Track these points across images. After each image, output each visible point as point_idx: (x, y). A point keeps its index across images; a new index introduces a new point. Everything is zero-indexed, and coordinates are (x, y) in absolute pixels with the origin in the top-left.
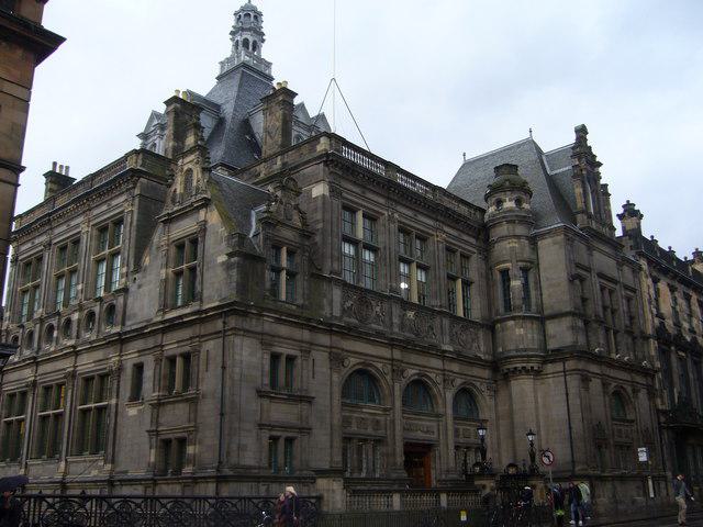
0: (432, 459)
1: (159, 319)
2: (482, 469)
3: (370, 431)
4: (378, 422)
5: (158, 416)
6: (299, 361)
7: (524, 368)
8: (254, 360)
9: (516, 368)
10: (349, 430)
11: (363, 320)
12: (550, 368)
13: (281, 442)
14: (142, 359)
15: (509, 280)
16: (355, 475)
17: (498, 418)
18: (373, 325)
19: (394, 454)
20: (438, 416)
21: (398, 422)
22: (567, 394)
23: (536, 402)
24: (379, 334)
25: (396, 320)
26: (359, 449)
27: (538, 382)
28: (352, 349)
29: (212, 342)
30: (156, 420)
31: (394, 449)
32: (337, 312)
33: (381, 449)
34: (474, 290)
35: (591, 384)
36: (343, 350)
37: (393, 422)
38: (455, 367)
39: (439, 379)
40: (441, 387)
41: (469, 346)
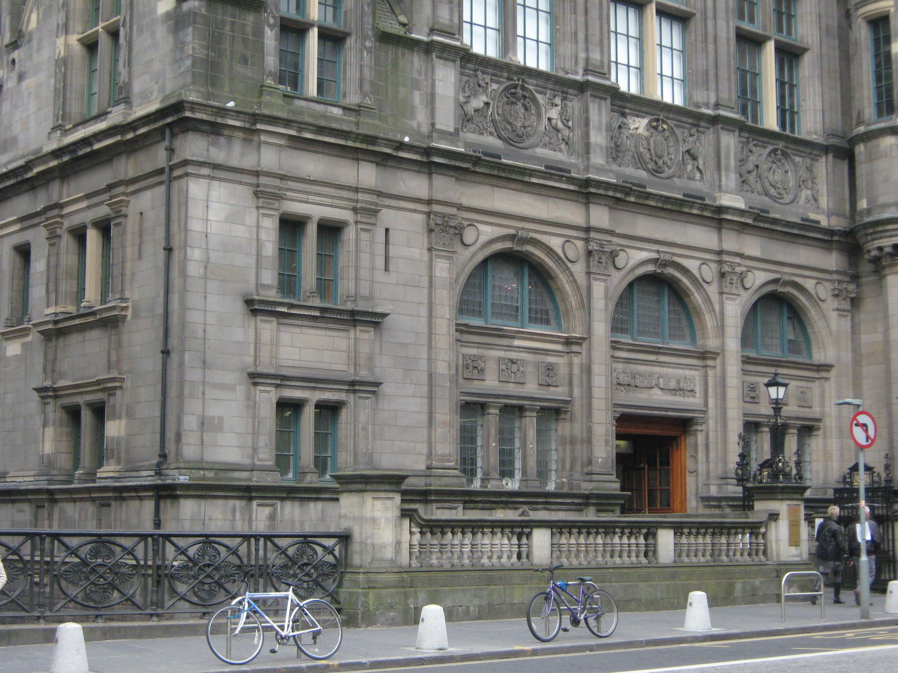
0: (689, 452)
1: (54, 146)
2: (774, 476)
3: (531, 388)
4: (550, 369)
5: (55, 360)
6: (350, 234)
8: (241, 232)
10: (476, 386)
11: (514, 139)
13: (308, 414)
14: (27, 236)
15: (888, 41)
16: (492, 486)
17: (857, 362)
18: (540, 152)
19: (589, 441)
20: (703, 355)
24: (555, 171)
25: (598, 138)
26: (505, 437)
29: (147, 196)
30: (51, 367)
31: (590, 430)
32: (446, 120)
33: (563, 428)
34: (807, 67)
36: (460, 207)
37: (588, 370)
38: (752, 246)
39: (709, 272)
40: (712, 290)
41: (788, 198)
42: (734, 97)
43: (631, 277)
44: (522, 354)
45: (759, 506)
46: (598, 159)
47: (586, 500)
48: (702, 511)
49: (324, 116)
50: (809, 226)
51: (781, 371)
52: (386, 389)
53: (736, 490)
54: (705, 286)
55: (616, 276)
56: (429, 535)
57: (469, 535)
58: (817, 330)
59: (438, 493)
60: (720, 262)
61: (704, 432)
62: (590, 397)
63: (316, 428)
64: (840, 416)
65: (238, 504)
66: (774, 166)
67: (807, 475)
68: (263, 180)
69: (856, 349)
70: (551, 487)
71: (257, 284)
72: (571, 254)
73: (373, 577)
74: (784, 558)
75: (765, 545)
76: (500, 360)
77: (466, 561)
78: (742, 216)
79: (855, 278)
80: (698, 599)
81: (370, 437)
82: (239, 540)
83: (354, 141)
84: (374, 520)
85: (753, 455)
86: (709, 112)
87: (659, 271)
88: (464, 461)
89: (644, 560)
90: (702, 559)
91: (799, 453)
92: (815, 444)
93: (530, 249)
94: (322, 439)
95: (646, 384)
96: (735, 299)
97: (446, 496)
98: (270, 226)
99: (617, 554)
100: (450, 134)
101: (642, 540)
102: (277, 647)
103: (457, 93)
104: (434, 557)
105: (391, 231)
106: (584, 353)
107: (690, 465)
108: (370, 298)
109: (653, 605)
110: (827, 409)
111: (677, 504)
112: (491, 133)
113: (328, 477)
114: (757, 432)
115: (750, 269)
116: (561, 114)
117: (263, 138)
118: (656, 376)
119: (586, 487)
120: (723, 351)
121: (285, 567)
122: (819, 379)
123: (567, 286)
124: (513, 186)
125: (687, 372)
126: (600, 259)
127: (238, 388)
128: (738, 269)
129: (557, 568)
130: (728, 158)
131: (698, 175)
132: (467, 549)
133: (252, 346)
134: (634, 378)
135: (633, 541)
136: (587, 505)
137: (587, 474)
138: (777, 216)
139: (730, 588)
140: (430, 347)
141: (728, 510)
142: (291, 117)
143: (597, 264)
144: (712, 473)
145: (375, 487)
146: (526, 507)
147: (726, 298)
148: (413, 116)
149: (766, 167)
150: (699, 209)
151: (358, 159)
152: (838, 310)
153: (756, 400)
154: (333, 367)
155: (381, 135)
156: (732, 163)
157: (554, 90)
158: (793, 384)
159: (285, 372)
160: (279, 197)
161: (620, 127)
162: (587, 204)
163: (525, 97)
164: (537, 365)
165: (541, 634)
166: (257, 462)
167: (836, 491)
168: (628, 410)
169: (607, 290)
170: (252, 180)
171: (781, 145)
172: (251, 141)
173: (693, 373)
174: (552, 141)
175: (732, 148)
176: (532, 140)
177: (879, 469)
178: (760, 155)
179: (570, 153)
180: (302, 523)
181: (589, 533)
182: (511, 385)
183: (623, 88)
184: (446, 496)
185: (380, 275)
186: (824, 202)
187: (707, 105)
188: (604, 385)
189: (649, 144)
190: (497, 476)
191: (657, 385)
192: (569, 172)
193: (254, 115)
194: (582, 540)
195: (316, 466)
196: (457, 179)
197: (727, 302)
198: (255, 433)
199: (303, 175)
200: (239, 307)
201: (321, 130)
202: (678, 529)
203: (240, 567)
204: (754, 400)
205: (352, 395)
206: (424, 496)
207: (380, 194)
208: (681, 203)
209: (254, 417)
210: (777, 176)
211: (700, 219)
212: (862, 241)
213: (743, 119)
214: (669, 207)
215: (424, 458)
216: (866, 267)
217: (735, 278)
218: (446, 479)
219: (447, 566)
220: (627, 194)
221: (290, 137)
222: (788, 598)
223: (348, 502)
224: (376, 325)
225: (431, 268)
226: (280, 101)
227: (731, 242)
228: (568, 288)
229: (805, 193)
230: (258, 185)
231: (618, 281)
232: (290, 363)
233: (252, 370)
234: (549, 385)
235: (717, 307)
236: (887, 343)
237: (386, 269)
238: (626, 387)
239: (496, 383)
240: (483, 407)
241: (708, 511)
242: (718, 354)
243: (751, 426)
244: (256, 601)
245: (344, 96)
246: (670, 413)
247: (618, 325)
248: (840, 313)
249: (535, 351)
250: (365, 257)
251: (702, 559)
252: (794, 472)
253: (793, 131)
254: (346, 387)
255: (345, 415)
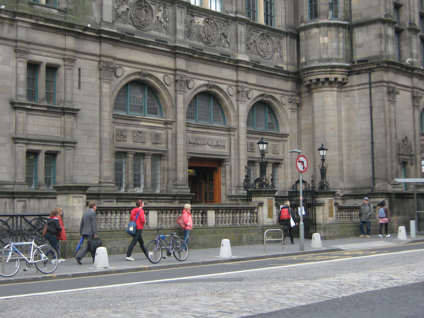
2: (261, 186)
3: (148, 145)
4: (157, 136)
6: (61, 71)
7: (327, 79)
8: (8, 69)
9: (318, 80)
10: (122, 144)
11: (141, 26)
12: (355, 79)
13: (42, 157)
16: (130, 191)
17: (299, 133)
18: (153, 32)
19: (176, 170)
20: (229, 130)
21: (180, 136)
22: (371, 108)
23: (339, 116)
24: (160, 42)
25: (180, 27)
26: (136, 168)
27: (343, 95)
28: (128, 58)
31: (176, 164)
32: (108, 17)
33: (163, 164)
35: (398, 96)
36: (115, 59)
37: (175, 136)
38: (252, 78)
39: (232, 91)
40: (233, 99)
42: (244, 8)
43: (196, 93)
44: (144, 129)
45: (254, 199)
46: (180, 37)
47: (174, 197)
48: (228, 202)
49: (49, 14)
50: (278, 69)
51: (265, 137)
52: (79, 145)
53: (243, 192)
54: (230, 97)
55: (189, 92)
56: (124, 214)
57: (119, 214)
58: (281, 118)
59: (104, 194)
60: (237, 86)
61: (229, 166)
62: (176, 149)
63: (45, 164)
64: (291, 158)
65: (8, 200)
66: (263, 41)
67: (277, 185)
68: (19, 44)
69: (299, 127)
70: (158, 191)
71: (16, 95)
72: (168, 82)
73: (73, 234)
74: (265, 223)
75: (257, 217)
76: (134, 131)
77: (118, 226)
78: (247, 65)
79: (299, 94)
80: (226, 242)
81: (72, 168)
82: (8, 217)
83: (64, 26)
84: (73, 208)
85: (252, 176)
86: (233, 15)
87: (209, 90)
88: (116, 179)
89: (201, 225)
90: (228, 224)
91: (273, 175)
92: (280, 171)
93: (148, 79)
94: (48, 169)
96: (244, 104)
97: (108, 196)
98: (22, 67)
99: (255, 221)
100: (110, 23)
101: (200, 216)
102: (27, 268)
103: (113, 4)
104: (102, 224)
105: (81, 70)
106: (174, 128)
107: (223, 181)
108: (71, 102)
109: (205, 246)
110: (286, 155)
111: (217, 199)
112: (130, 24)
113: (51, 187)
114: (254, 165)
115: (251, 89)
116: (163, 15)
117: (19, 24)
118: (207, 139)
119: (174, 191)
120: (238, 127)
121: (30, 230)
122: (282, 141)
123: (165, 97)
124: (140, 49)
125: (221, 137)
126: (242, 94)
127: (7, 145)
128: (246, 90)
129: (160, 229)
130: (241, 37)
131: (227, 45)
132: (118, 221)
133: (14, 124)
135: (196, 216)
136: (175, 200)
137: (175, 185)
138: (264, 65)
139: (241, 237)
140: (100, 125)
141: (240, 202)
142: (33, 14)
143: (179, 86)
144: (233, 185)
145: (74, 192)
146: (146, 201)
148: (92, 15)
149: (258, 42)
150: (227, 61)
151: (65, 35)
152: (291, 109)
153: (253, 151)
154: (54, 135)
155: (77, 23)
156: (243, 39)
157: (160, 3)
158: (270, 143)
159: (30, 137)
160: (27, 53)
161: (191, 22)
162: (175, 58)
163: (146, 6)
164: (151, 134)
165: (153, 260)
166: (16, 181)
167: (289, 192)
168: (194, 155)
169: (184, 98)
170: (14, 44)
171: (266, 31)
172: (13, 25)
173: (224, 138)
174: (159, 28)
175: (243, 32)
176: (149, 27)
177: (309, 182)
178: (256, 36)
179: (167, 33)
180: (39, 210)
181: (175, 213)
182: (139, 143)
183: (192, 3)
184: (108, 196)
185: (76, 91)
186: (285, 58)
187: (232, 12)
188: (183, 143)
189: (204, 30)
190: (132, 186)
191: (208, 144)
192: (167, 42)
193: (14, 12)
194: (172, 216)
195: (46, 182)
196: (113, 45)
197: (240, 105)
198: (16, 166)
199: (39, 42)
200: (8, 105)
201: (47, 20)
202: (217, 210)
203: (8, 231)
204: (252, 150)
205: (63, 148)
206: (98, 196)
207: (76, 52)
208: (219, 58)
209: (15, 158)
210: (264, 46)
211: (228, 66)
212: (302, 77)
213: (248, 19)
214: (214, 60)
215: (97, 178)
216: (304, 89)
217: (244, 93)
218: (108, 188)
219: (109, 229)
220: (194, 53)
221: (32, 24)
222: (267, 242)
223: (61, 199)
224: (74, 115)
225: (101, 87)
226: (27, 6)
227: (242, 76)
228: (166, 97)
229: (277, 54)
230: (16, 47)
231: (190, 94)
232: (33, 133)
233: (14, 136)
234: (157, 144)
235: (235, 107)
236: (313, 124)
237: (79, 88)
238: (193, 144)
239: (132, 143)
240: (125, 154)
241: (231, 202)
242: (236, 129)
243: (251, 163)
244: (17, 246)
245: (59, 4)
246: (214, 157)
247: (190, 115)
248: (292, 110)
249: (150, 127)
250: (69, 82)
251: (228, 224)
252: (270, 184)
253: (271, 25)
254: (60, 144)
255: (59, 157)
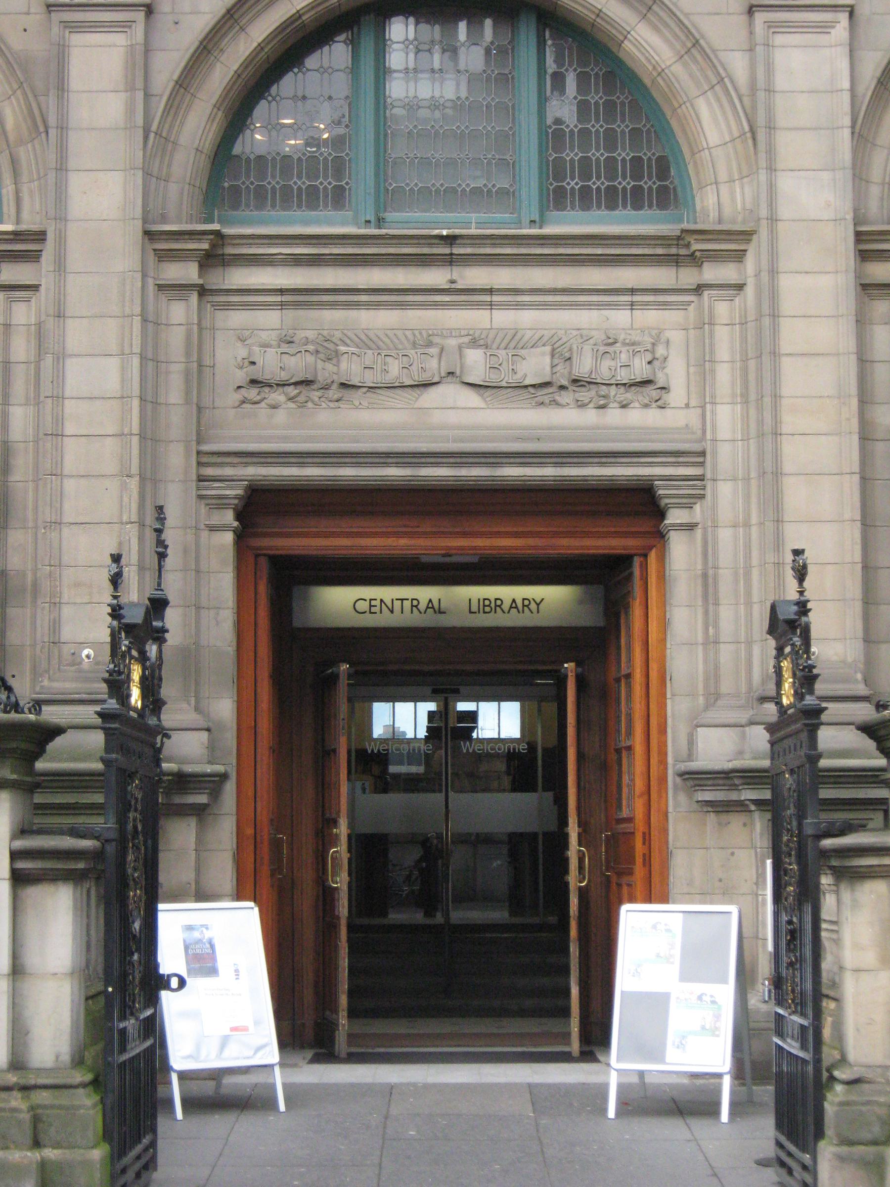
61: (699, 532)
95: (369, 379)
96: (824, 28)
118: (453, 342)
125: (620, 318)
134: (333, 356)
147: (769, 24)
168: (464, 472)
173: (650, 317)
197: (779, 39)
238: (292, 391)
242: (746, 235)
